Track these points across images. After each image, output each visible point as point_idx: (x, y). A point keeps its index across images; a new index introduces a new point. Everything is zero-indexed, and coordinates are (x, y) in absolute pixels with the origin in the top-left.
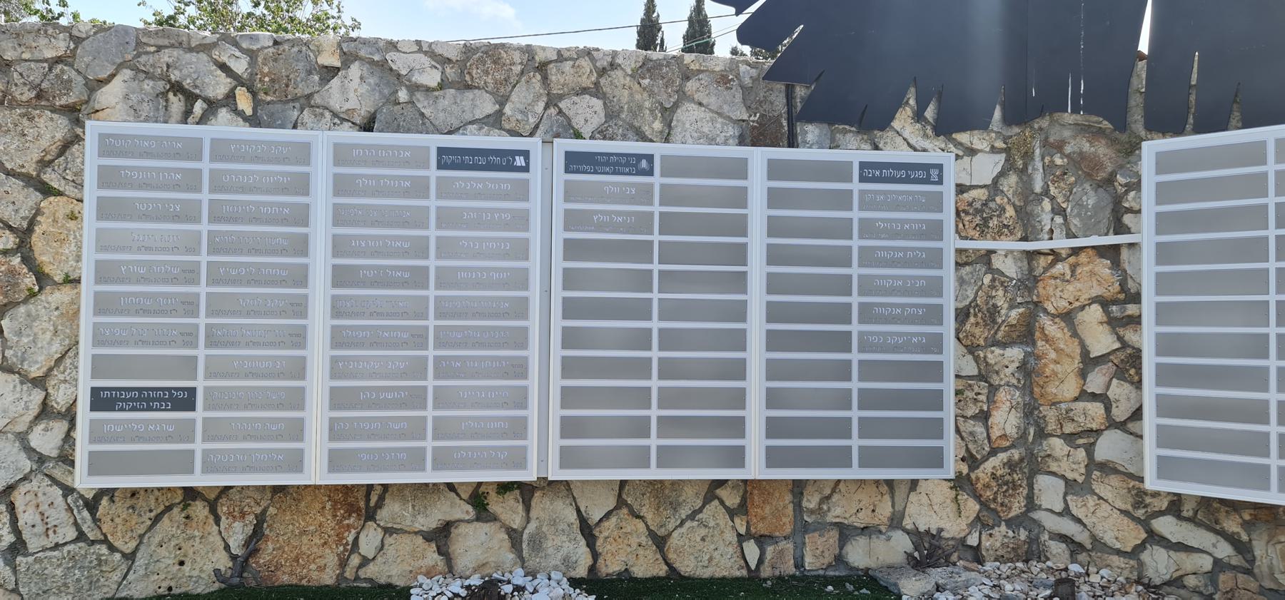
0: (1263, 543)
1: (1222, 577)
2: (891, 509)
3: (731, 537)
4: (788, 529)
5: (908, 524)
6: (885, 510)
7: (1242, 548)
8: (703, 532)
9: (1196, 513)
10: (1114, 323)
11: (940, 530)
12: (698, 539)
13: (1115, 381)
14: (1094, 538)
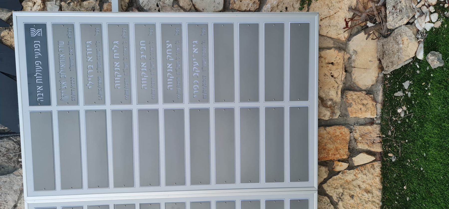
2: (332, 50)
3: (350, 176)
4: (345, 130)
5: (344, 36)
6: (333, 55)
8: (347, 197)
11: (350, 9)
12: (352, 201)
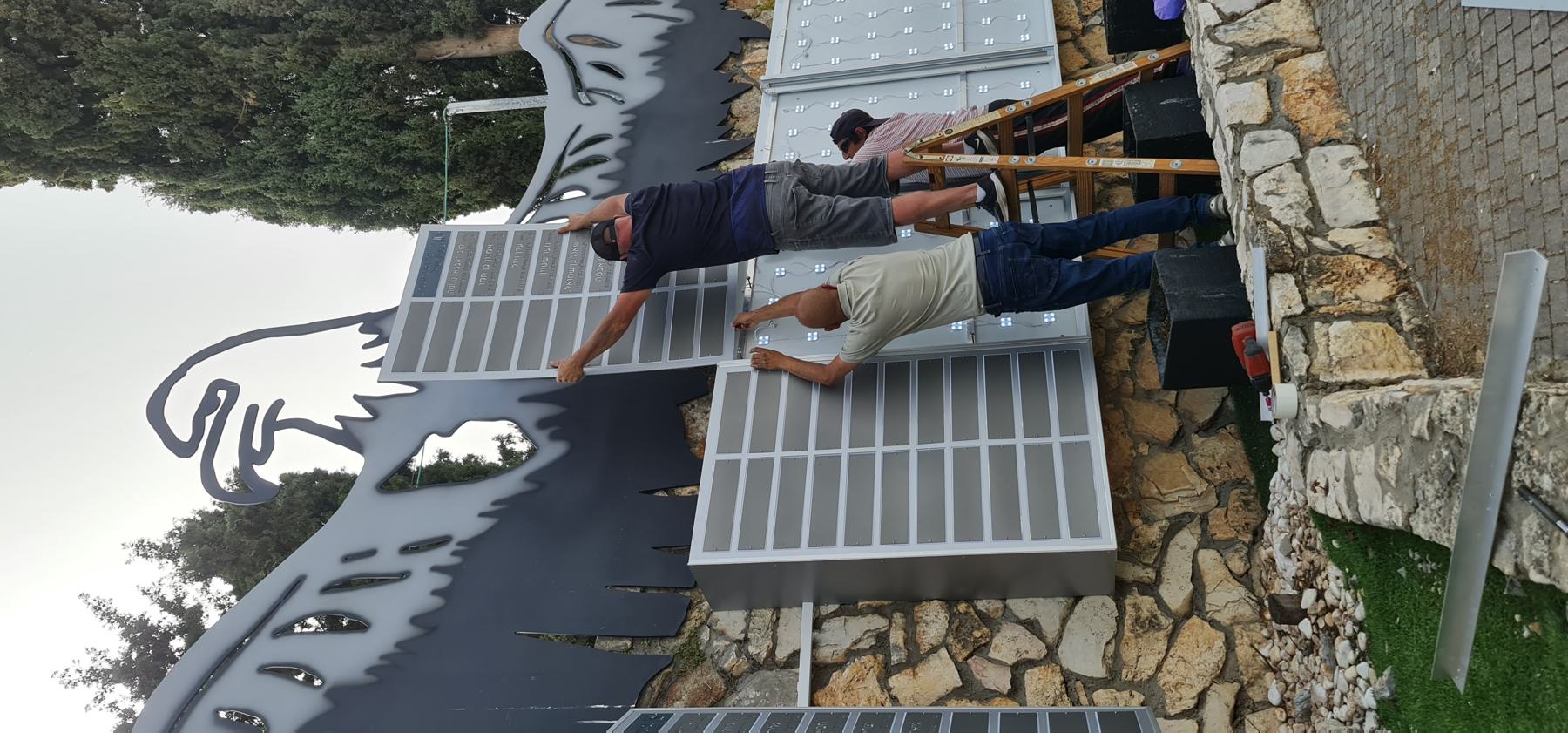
0: (1165, 507)
1: (1219, 536)
7: (1176, 525)
9: (1147, 565)
10: (915, 658)
13: (992, 654)
14: (1221, 676)
